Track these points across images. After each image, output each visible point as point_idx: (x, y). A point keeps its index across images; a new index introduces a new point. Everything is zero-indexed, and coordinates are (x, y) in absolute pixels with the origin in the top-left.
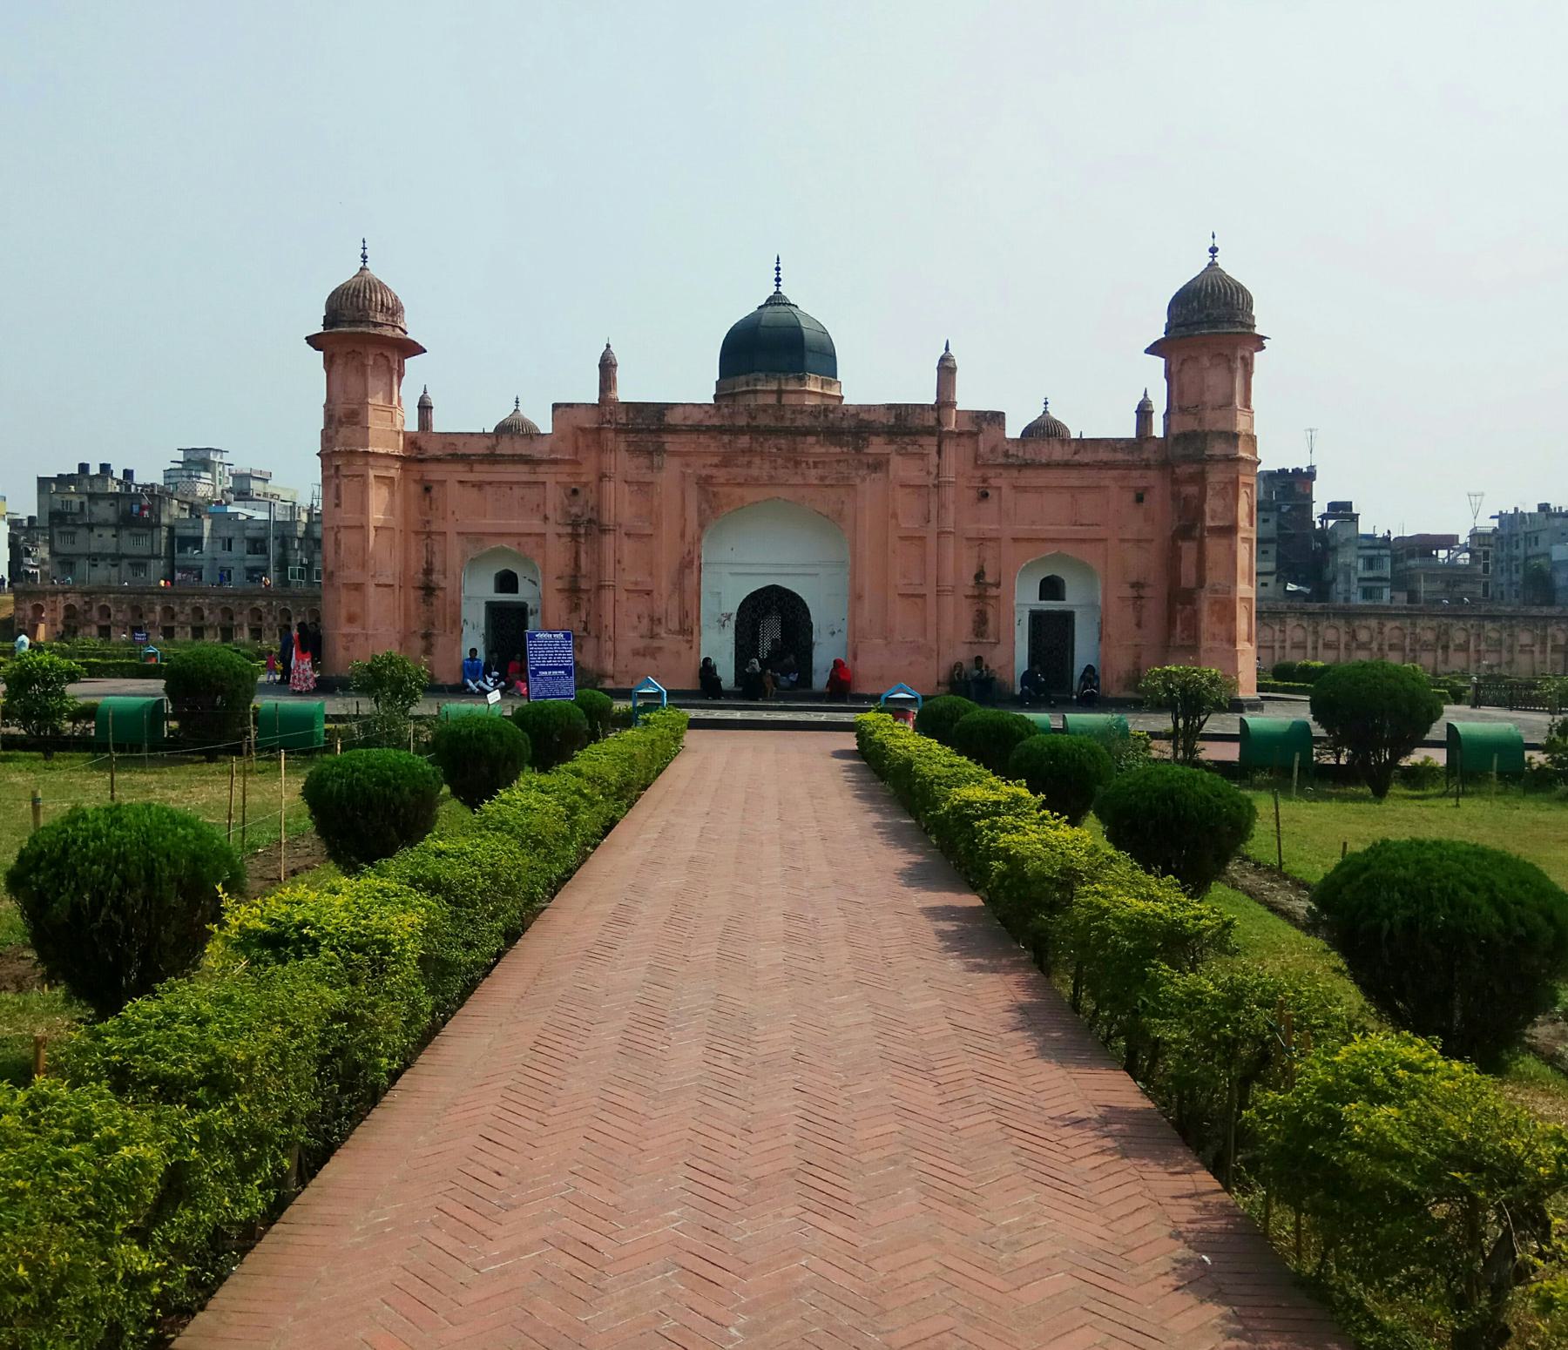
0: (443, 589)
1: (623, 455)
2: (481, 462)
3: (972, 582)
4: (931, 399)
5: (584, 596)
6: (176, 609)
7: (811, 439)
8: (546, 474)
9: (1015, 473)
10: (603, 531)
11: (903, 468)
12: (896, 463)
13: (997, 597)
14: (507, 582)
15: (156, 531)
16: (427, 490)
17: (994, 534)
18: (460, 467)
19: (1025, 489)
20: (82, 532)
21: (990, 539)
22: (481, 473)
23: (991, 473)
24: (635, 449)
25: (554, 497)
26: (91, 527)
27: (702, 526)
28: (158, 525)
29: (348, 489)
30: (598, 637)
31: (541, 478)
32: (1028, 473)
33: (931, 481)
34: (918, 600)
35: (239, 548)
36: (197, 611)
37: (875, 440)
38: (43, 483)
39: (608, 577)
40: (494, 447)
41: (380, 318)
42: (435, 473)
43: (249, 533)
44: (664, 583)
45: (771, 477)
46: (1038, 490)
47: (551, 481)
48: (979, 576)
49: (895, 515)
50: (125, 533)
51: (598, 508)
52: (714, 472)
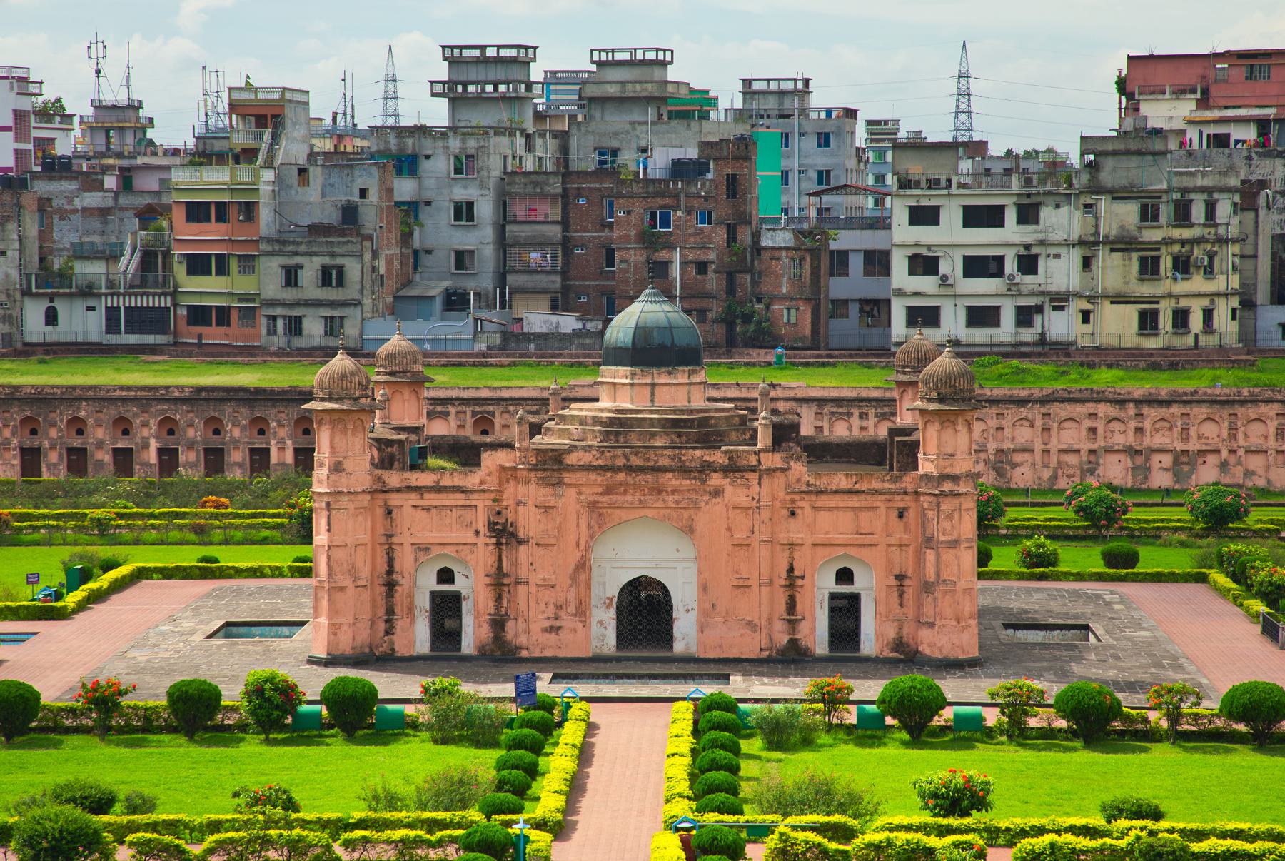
1: (532, 487)
2: (429, 492)
3: (784, 575)
5: (506, 589)
7: (670, 475)
9: (813, 498)
10: (520, 542)
14: (446, 576)
16: (390, 512)
17: (799, 541)
18: (413, 496)
19: (820, 509)
22: (431, 500)
23: (797, 497)
24: (543, 482)
27: (591, 536)
31: (474, 503)
32: (824, 497)
33: (754, 504)
37: (715, 475)
39: (522, 574)
41: (357, 393)
42: (395, 500)
45: (641, 502)
46: (830, 509)
47: (480, 505)
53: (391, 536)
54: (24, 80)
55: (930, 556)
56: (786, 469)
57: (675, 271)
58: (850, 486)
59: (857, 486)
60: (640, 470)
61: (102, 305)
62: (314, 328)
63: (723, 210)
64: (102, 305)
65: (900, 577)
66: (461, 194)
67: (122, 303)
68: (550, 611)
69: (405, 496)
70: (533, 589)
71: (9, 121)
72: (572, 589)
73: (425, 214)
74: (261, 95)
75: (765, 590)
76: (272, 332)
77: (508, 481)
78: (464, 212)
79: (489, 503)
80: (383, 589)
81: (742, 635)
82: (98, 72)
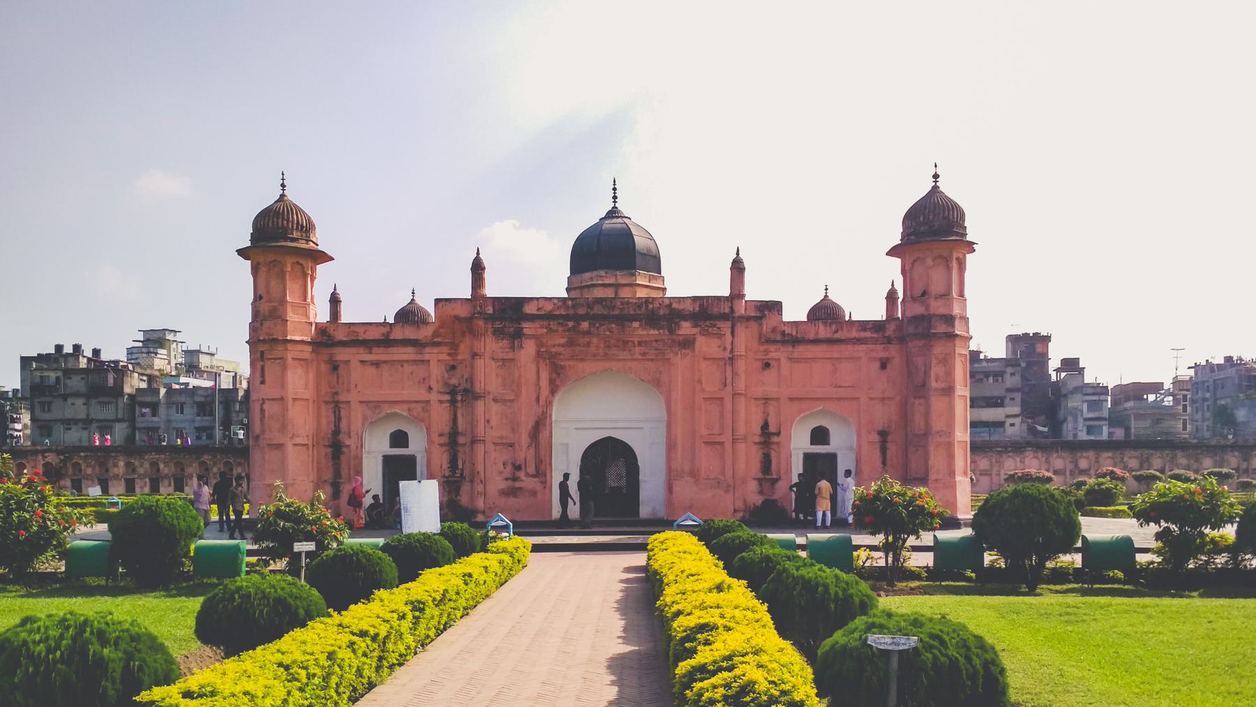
0: (348, 446)
3: (759, 431)
4: (726, 292)
6: (137, 463)
7: (636, 324)
9: (790, 349)
10: (477, 397)
11: (706, 345)
12: (701, 342)
13: (778, 443)
16: (335, 367)
17: (775, 396)
18: (361, 350)
20: (58, 403)
21: (772, 399)
22: (378, 354)
25: (436, 371)
26: (65, 397)
28: (121, 394)
29: (271, 370)
30: (472, 481)
31: (427, 357)
33: (727, 354)
34: (718, 447)
35: (189, 412)
36: (154, 464)
38: (25, 361)
40: (389, 333)
42: (342, 354)
43: (198, 399)
44: (525, 440)
46: (806, 360)
48: (765, 426)
49: (700, 382)
50: (93, 402)
51: (471, 380)
52: (561, 349)
53: (336, 393)
55: (918, 406)
56: (761, 318)
58: (829, 336)
59: (837, 336)
65: (883, 434)
68: (509, 470)
69: (353, 350)
70: (491, 448)
72: (532, 450)
77: (463, 334)
79: (445, 357)
80: (329, 450)
81: (714, 496)
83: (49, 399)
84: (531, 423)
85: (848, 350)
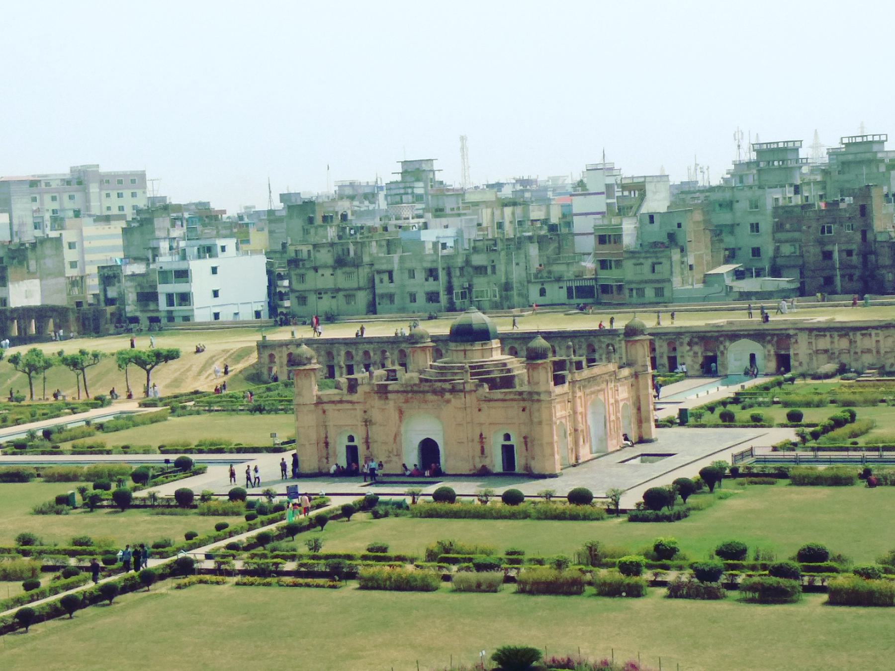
6: (354, 352)
8: (357, 406)
12: (453, 400)
15: (360, 269)
16: (324, 412)
19: (493, 407)
20: (310, 274)
22: (339, 406)
24: (380, 398)
25: (359, 413)
26: (316, 269)
35: (420, 276)
36: (366, 353)
42: (326, 407)
48: (481, 435)
50: (339, 272)
54: (612, 169)
57: (836, 255)
60: (416, 392)
61: (565, 285)
62: (650, 293)
63: (858, 223)
64: (565, 285)
65: (525, 438)
66: (753, 219)
67: (574, 284)
71: (603, 189)
73: (737, 230)
74: (635, 181)
75: (470, 444)
76: (631, 296)
78: (755, 227)
82: (739, 146)
83: (302, 271)
84: (393, 435)
85: (508, 403)
